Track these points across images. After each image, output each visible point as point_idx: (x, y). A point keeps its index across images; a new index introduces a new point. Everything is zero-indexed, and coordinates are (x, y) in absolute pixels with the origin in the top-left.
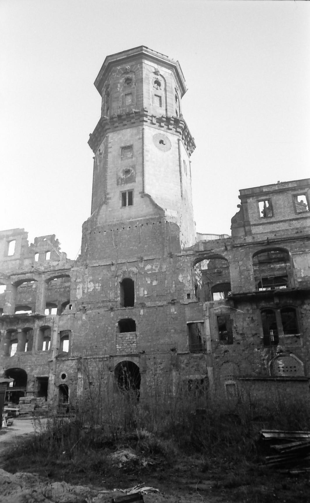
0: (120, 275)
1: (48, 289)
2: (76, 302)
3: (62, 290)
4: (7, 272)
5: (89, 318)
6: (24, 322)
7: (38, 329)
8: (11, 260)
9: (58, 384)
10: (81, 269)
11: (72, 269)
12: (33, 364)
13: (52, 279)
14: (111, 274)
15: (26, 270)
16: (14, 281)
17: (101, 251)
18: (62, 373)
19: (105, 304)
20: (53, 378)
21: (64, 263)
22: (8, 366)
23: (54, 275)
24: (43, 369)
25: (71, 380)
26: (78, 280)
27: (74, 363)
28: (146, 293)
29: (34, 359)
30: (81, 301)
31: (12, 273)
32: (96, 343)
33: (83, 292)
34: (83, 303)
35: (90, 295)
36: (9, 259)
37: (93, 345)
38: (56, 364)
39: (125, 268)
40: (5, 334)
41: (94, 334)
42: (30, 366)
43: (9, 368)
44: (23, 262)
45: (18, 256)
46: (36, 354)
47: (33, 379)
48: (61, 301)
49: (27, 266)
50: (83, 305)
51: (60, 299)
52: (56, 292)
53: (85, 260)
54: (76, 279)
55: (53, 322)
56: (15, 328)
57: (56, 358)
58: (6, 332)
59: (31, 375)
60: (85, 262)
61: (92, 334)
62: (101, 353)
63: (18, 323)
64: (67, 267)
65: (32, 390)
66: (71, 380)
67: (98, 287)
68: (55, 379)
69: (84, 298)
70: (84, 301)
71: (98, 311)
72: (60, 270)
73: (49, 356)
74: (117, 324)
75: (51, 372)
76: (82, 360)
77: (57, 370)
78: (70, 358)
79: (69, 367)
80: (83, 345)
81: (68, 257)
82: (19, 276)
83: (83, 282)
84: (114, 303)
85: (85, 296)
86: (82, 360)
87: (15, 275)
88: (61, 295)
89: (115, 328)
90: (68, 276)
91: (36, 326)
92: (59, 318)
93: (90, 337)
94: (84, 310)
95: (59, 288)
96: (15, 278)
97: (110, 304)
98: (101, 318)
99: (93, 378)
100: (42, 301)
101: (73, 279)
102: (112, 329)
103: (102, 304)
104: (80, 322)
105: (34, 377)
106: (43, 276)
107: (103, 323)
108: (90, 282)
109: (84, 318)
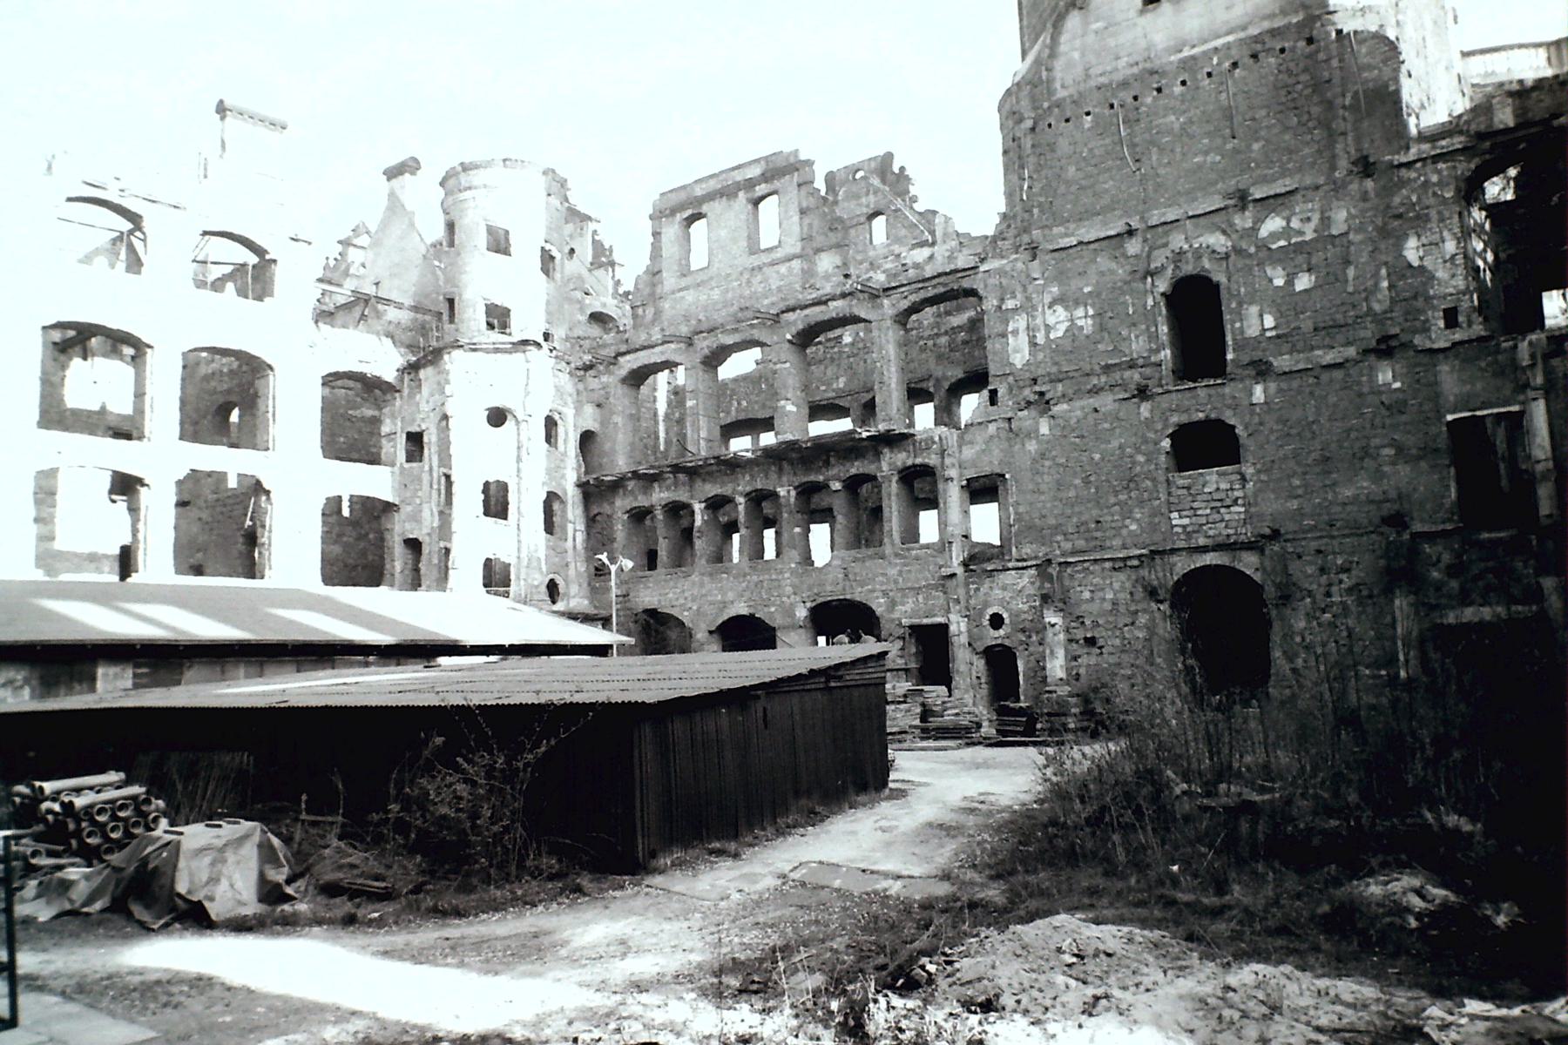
0: (1163, 267)
1: (904, 344)
2: (1011, 379)
3: (943, 340)
4: (766, 302)
8: (773, 264)
9: (980, 646)
10: (1015, 262)
13: (915, 308)
14: (1128, 268)
15: (827, 289)
17: (1082, 188)
18: (991, 611)
20: (963, 627)
23: (922, 295)
28: (1269, 321)
31: (782, 306)
32: (1095, 512)
33: (1033, 344)
34: (1035, 381)
35: (1055, 348)
36: (765, 258)
39: (1178, 241)
42: (885, 594)
46: (897, 555)
48: (945, 378)
50: (1037, 388)
51: (938, 372)
52: (923, 350)
53: (1026, 230)
54: (1002, 300)
55: (942, 453)
57: (965, 564)
60: (1026, 239)
61: (1078, 482)
64: (963, 261)
67: (1084, 319)
68: (969, 631)
70: (1040, 372)
71: (1093, 402)
72: (939, 275)
74: (1166, 444)
75: (955, 608)
77: (972, 602)
78: (1010, 565)
80: (1052, 521)
83: (1028, 308)
84: (1148, 371)
87: (793, 309)
88: (940, 357)
89: (1163, 458)
90: (972, 293)
93: (1072, 493)
94: (1043, 403)
95: (930, 337)
96: (797, 320)
97: (1135, 376)
100: (893, 386)
101: (990, 303)
102: (1148, 461)
103: (1103, 379)
104: (1032, 446)
106: (886, 302)
109: (1044, 429)
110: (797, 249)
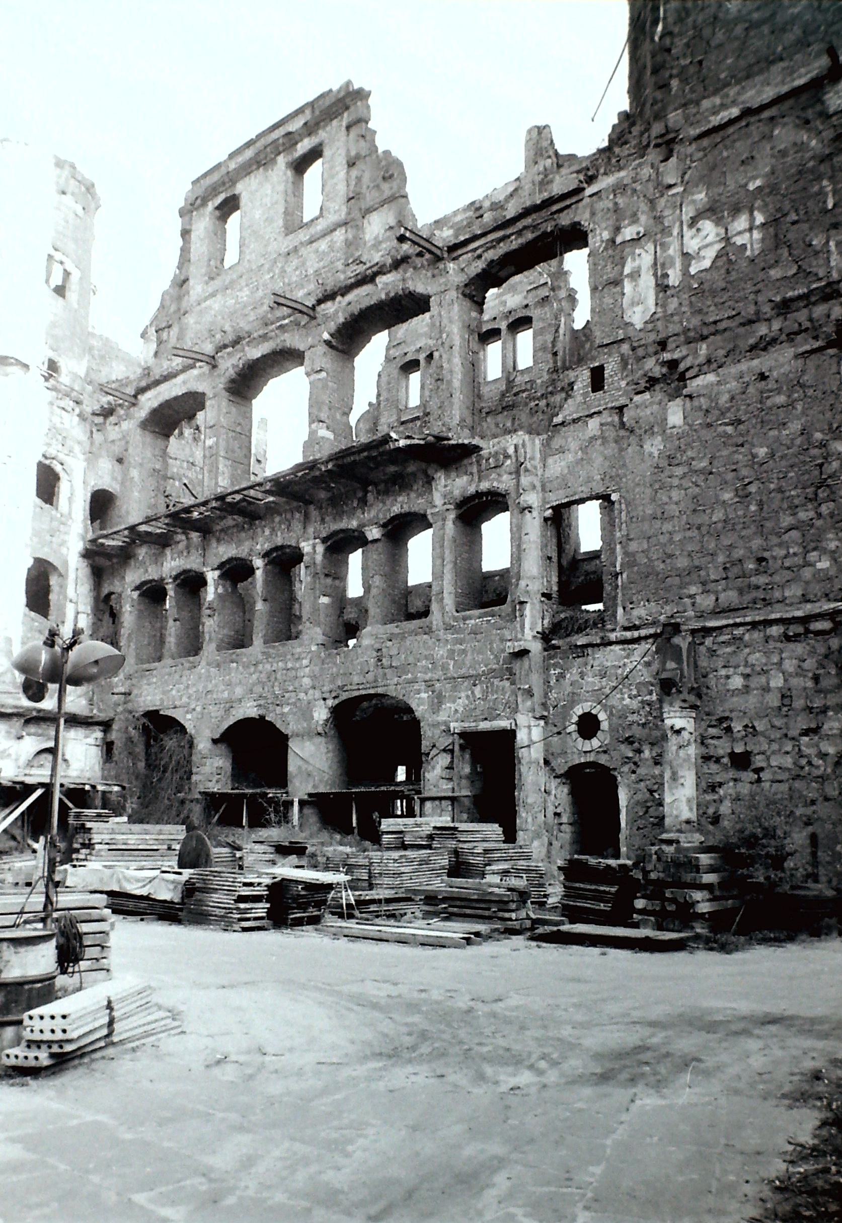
2: (625, 348)
5: (709, 415)
6: (387, 492)
7: (452, 516)
11: (589, 191)
12: (439, 674)
15: (377, 257)
16: (333, 326)
18: (579, 710)
19: (802, 316)
20: (537, 733)
21: (546, 172)
22: (341, 688)
24: (485, 693)
25: (629, 741)
26: (628, 233)
27: (636, 657)
29: (441, 652)
30: (652, 337)
32: (757, 543)
33: (662, 287)
34: (663, 345)
35: (699, 290)
37: (739, 553)
38: (547, 669)
40: (319, 558)
41: (743, 496)
42: (429, 684)
43: (344, 696)
44: (359, 228)
45: (338, 211)
46: (448, 628)
47: (444, 742)
49: (377, 245)
50: (667, 356)
54: (617, 230)
56: (354, 524)
57: (545, 637)
58: (320, 549)
59: (436, 725)
61: (727, 496)
62: (793, 591)
63: (363, 502)
65: (445, 789)
66: (629, 741)
67: (747, 232)
69: (668, 318)
70: (674, 328)
72: (527, 212)
73: (507, 634)
75: (525, 704)
76: (682, 642)
77: (553, 695)
78: (613, 636)
79: (613, 675)
80: (682, 562)
81: (563, 149)
82: (350, 297)
85: (673, 304)
86: (682, 642)
91: (438, 500)
92: (546, 444)
93: (718, 515)
94: (674, 378)
98: (781, 399)
99: (751, 731)
100: (456, 383)
104: (654, 446)
105: (448, 731)
106: (451, 266)
107: (795, 426)
108: (693, 222)
110: (343, 215)
